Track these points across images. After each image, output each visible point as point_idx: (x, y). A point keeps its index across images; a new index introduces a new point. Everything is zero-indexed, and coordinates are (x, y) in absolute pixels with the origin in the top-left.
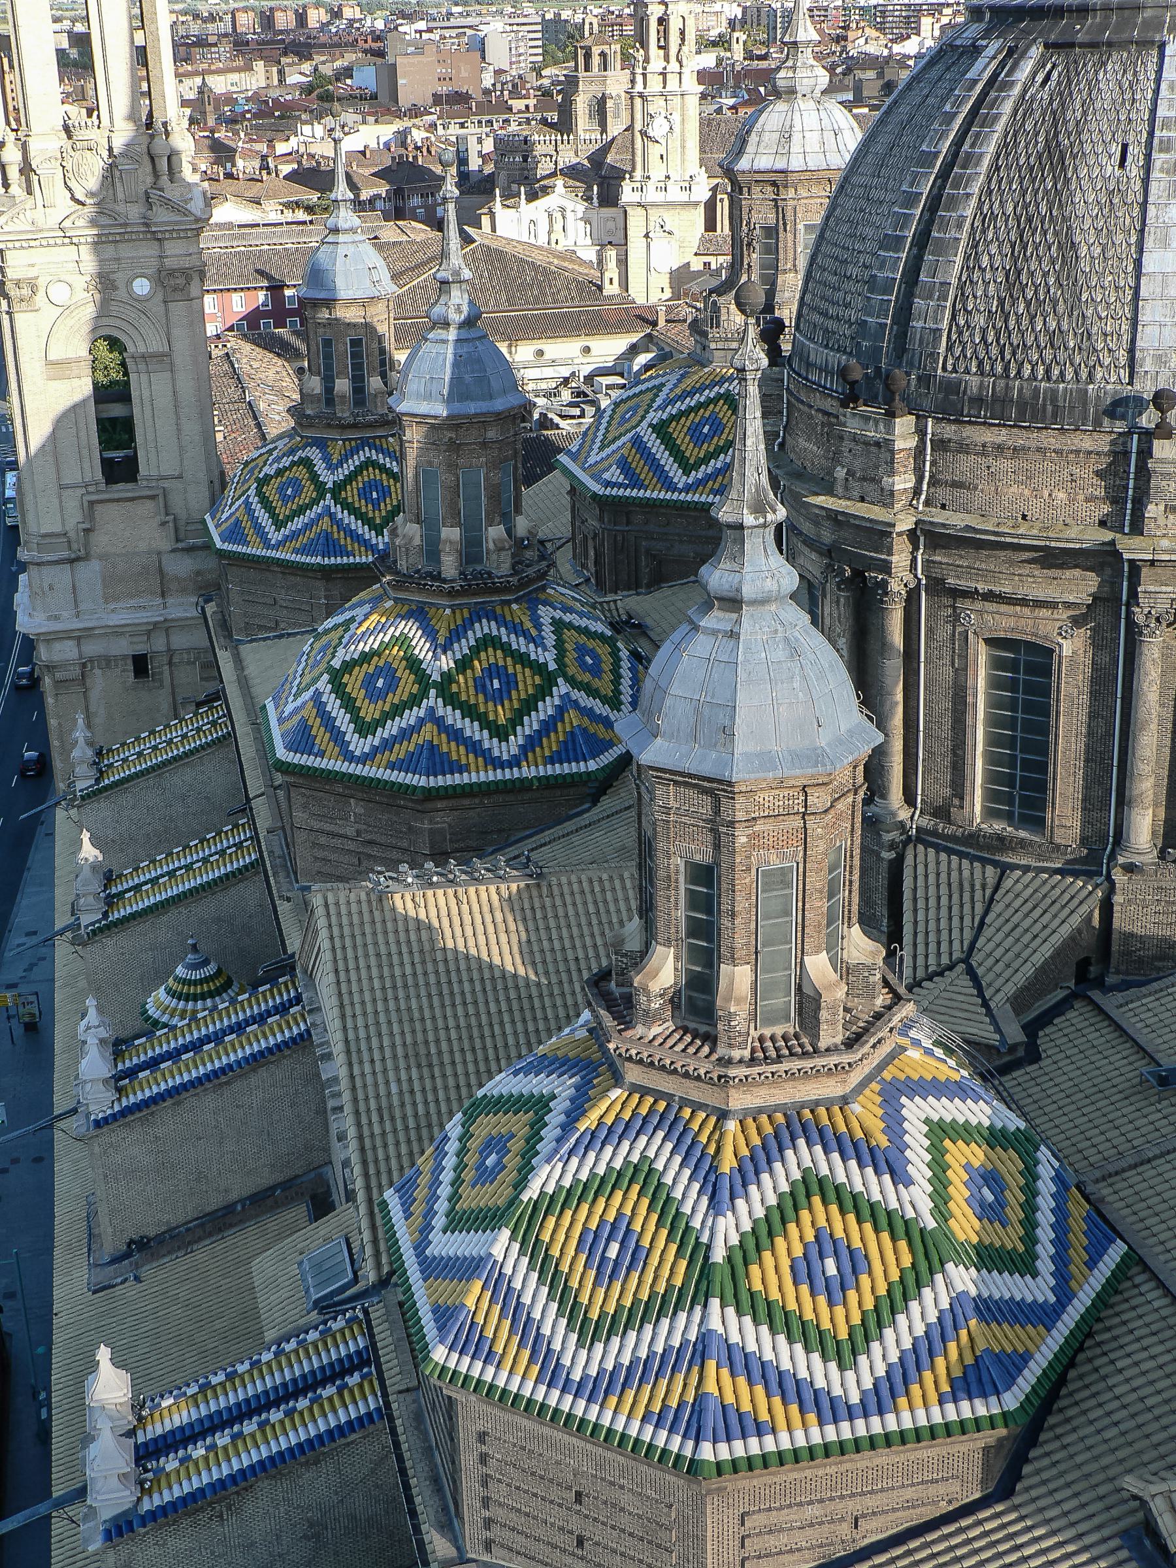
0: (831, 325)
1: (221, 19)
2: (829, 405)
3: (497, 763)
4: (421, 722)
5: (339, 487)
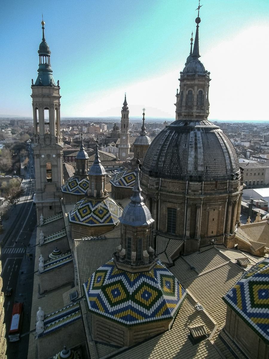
0: (148, 165)
2: (147, 176)
3: (100, 223)
4: (90, 217)
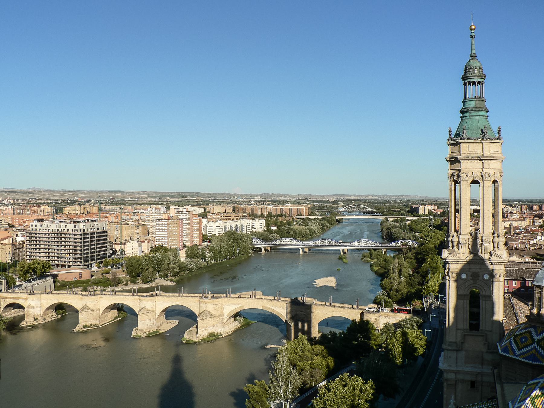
1: (518, 207)
5: (539, 342)
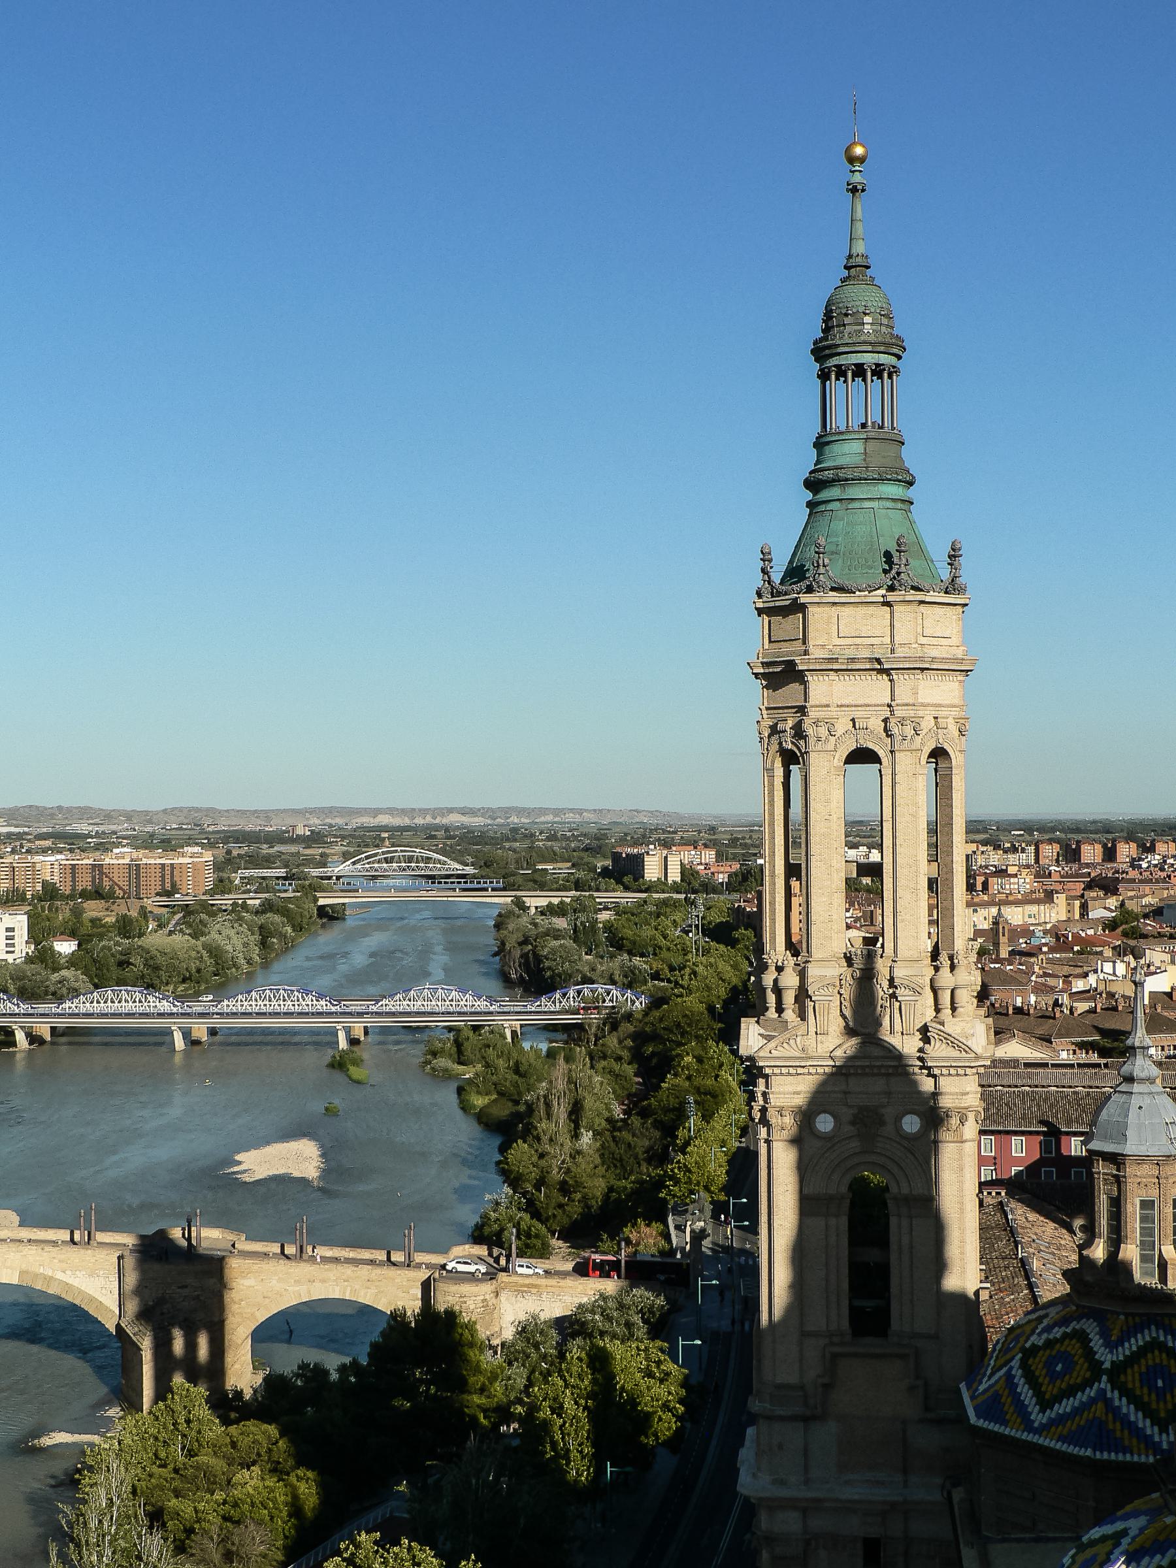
1: (1023, 851)
5: (1117, 1370)
